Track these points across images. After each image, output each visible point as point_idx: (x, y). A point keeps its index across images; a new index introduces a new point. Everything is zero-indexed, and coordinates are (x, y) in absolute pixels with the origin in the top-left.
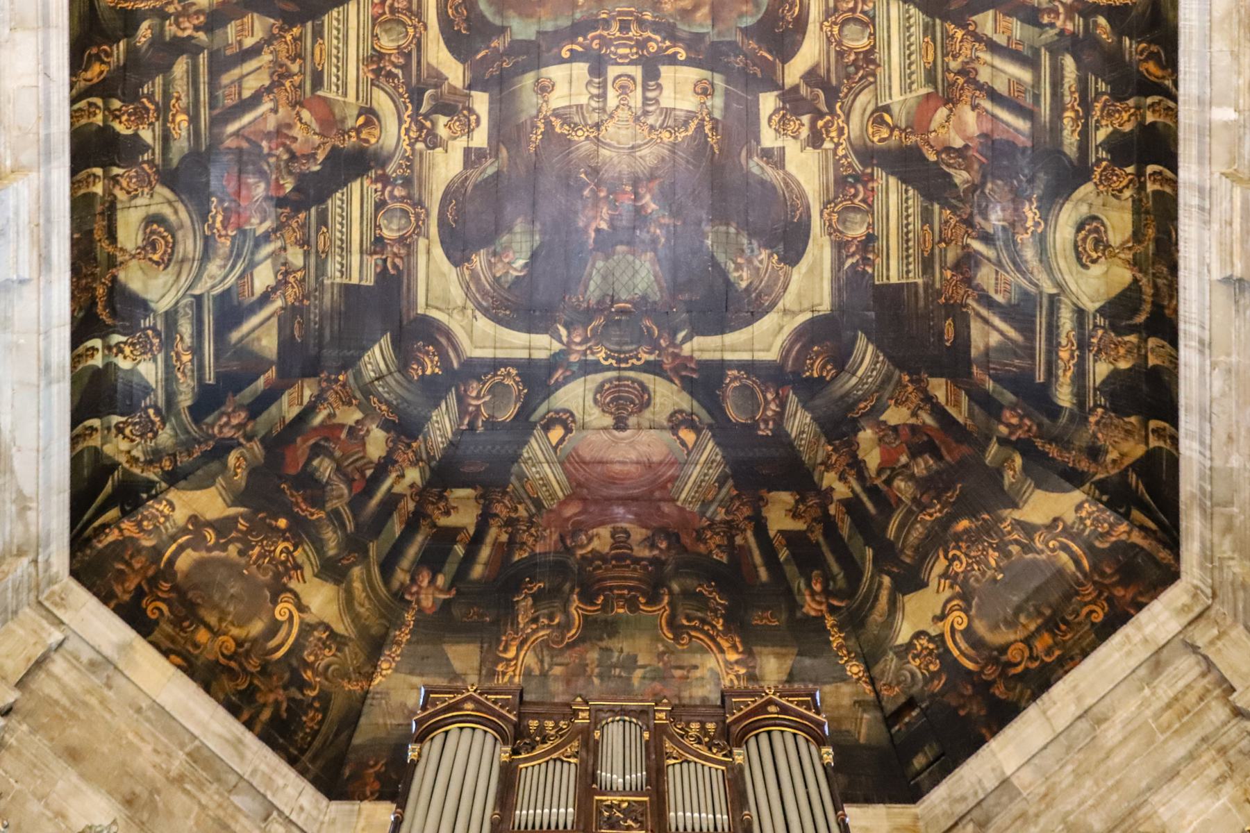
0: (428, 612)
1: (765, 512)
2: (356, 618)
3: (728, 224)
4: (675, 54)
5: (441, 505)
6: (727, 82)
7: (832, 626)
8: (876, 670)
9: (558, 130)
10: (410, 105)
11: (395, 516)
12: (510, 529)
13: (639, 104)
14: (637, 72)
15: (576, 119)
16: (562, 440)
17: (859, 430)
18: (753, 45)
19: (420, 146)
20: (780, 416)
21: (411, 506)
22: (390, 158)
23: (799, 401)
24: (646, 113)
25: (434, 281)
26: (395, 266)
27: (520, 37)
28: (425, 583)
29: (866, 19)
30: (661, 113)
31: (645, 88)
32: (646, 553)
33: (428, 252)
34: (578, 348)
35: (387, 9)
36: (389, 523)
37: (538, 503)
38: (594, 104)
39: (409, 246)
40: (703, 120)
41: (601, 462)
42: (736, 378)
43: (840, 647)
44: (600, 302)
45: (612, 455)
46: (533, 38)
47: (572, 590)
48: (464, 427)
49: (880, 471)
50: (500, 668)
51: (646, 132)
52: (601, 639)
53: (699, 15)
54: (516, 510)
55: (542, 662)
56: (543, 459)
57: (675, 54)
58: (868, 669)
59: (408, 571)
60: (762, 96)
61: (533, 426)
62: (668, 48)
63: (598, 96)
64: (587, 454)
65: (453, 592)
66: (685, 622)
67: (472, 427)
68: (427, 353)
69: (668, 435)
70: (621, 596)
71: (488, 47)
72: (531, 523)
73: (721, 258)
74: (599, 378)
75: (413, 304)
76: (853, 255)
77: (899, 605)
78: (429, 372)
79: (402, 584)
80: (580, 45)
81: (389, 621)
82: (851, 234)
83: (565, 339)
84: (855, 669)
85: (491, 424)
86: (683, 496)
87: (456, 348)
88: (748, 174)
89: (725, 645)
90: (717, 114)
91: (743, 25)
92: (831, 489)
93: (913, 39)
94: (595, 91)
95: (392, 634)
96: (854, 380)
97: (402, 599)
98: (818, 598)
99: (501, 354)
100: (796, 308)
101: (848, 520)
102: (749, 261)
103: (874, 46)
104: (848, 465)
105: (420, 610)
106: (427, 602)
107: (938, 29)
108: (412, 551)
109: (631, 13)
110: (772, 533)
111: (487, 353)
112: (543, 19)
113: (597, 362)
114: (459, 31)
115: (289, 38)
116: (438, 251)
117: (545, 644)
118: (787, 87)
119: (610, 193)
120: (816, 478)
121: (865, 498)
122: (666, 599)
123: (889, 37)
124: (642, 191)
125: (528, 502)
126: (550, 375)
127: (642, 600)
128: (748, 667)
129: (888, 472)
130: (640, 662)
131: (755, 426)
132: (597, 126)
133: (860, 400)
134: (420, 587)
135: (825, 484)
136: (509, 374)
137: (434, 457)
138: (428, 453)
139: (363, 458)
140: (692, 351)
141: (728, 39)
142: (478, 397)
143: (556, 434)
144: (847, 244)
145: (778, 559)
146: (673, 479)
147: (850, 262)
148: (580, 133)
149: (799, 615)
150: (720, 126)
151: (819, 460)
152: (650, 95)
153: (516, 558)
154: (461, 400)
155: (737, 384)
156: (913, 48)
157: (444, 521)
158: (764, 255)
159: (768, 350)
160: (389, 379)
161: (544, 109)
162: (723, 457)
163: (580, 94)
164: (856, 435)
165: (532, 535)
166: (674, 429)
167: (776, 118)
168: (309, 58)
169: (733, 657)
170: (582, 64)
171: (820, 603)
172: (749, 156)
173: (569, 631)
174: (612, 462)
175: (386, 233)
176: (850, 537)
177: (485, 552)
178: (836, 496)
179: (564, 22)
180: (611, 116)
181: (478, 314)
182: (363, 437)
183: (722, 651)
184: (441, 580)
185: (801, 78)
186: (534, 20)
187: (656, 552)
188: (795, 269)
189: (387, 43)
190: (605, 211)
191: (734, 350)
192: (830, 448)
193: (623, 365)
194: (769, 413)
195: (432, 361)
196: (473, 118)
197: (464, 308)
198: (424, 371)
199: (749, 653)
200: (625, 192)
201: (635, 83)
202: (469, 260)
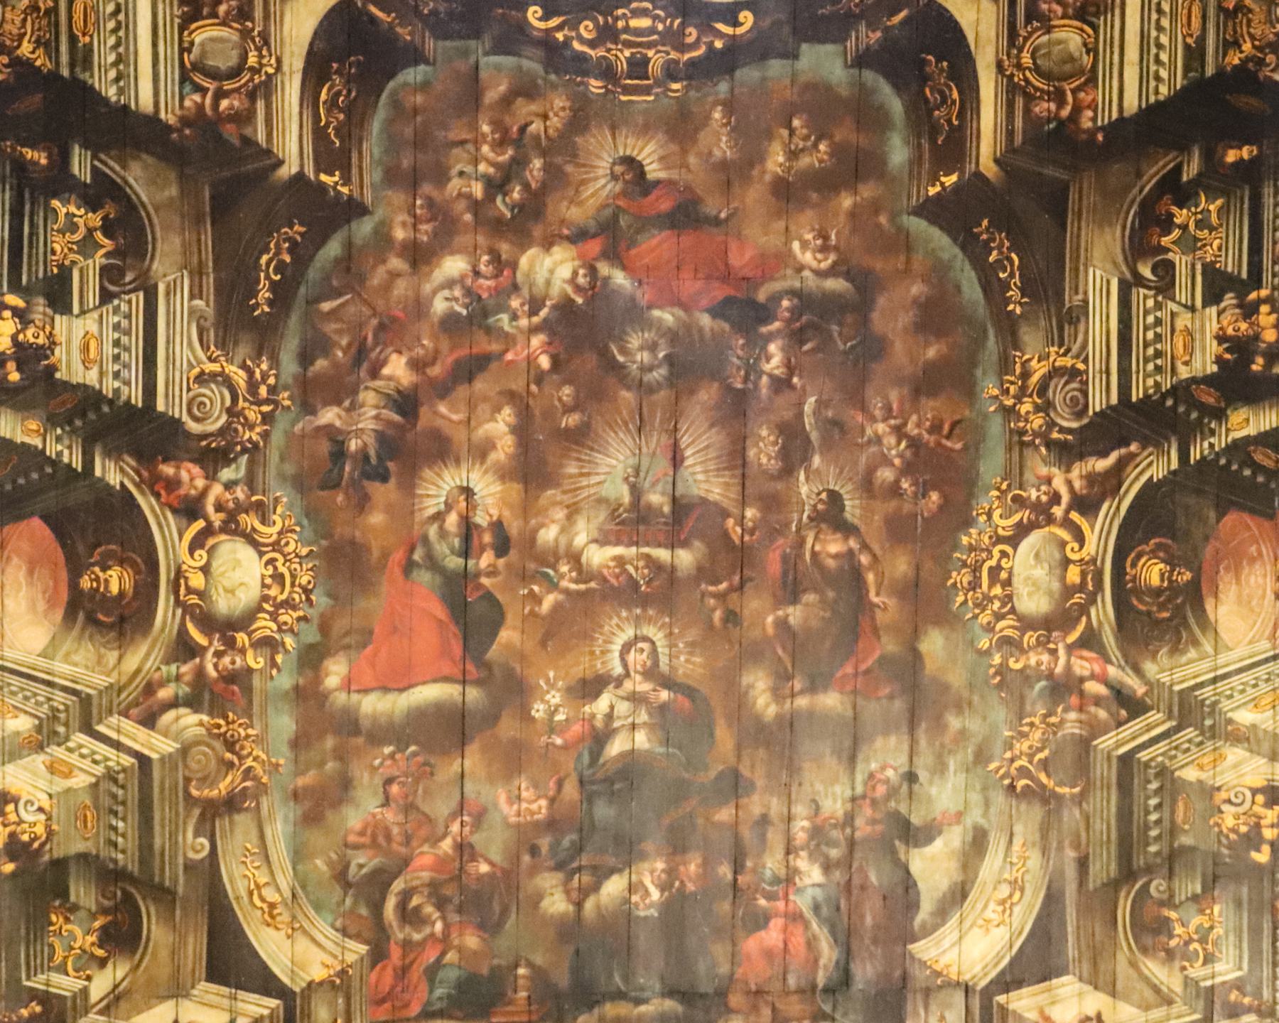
18: (404, 32)
27: (830, 48)
29: (198, 78)
35: (1070, 98)
46: (804, 47)
53: (503, 88)
62: (560, 28)
71: (887, 30)
80: (720, 35)
91: (422, 67)
93: (112, 41)
103: (182, 29)
107: (64, 58)
109: (628, 90)
112: (787, 82)
114: (939, 60)
115: (1247, 47)
123: (155, 45)
141: (448, 43)
156: (111, 25)
168: (1211, 12)
179: (748, 74)
189: (1070, 38)
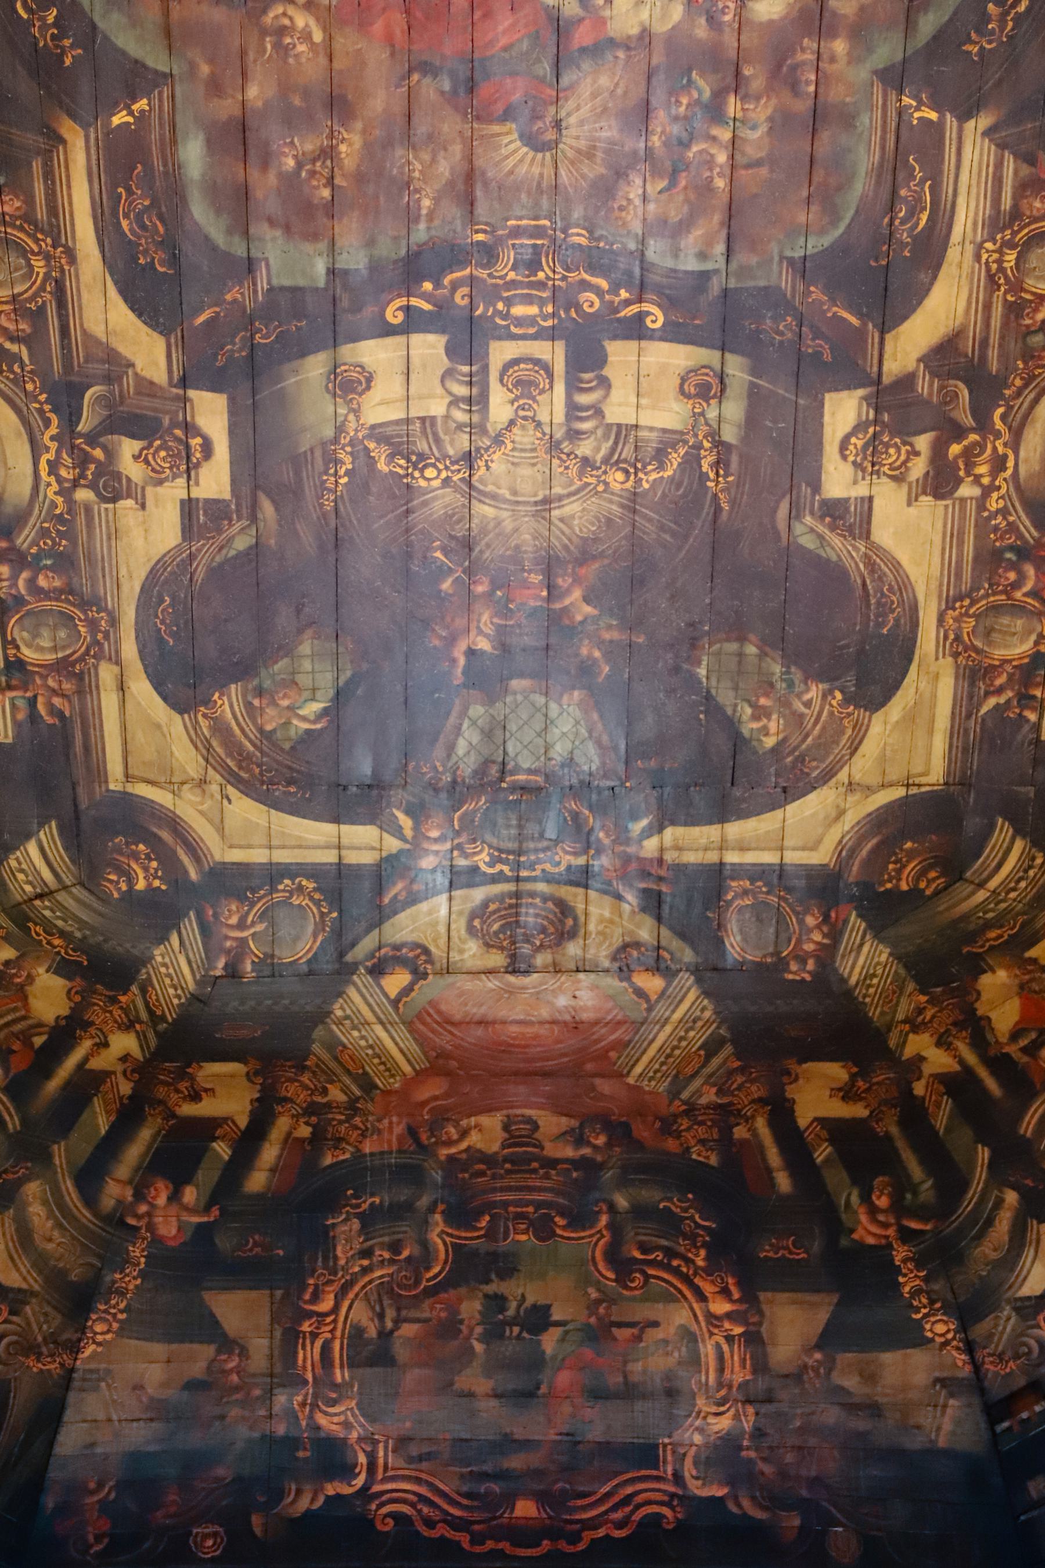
0: (172, 1243)
1: (791, 1091)
2: (40, 1262)
3: (742, 639)
4: (641, 317)
5: (183, 1086)
6: (754, 372)
7: (905, 1261)
8: (979, 1330)
9: (382, 466)
10: (55, 420)
11: (97, 1103)
12: (314, 1119)
13: (559, 417)
14: (555, 353)
15: (422, 446)
16: (407, 990)
17: (984, 972)
19: (83, 495)
20: (827, 955)
21: (126, 1088)
22: (21, 518)
23: (870, 926)
24: (574, 435)
25: (139, 737)
26: (52, 710)
28: (162, 1200)
30: (606, 436)
31: (573, 386)
32: (569, 1152)
33: (122, 688)
34: (435, 847)
36: (85, 1116)
37: (368, 1085)
38: (460, 416)
39: (80, 677)
40: (699, 447)
41: (482, 1022)
42: (745, 892)
43: (916, 1293)
44: (481, 772)
45: (502, 1013)
47: (432, 1209)
48: (218, 973)
49: (1015, 1035)
50: (306, 1327)
51: (574, 471)
52: (488, 1281)
54: (325, 1092)
55: (381, 1316)
56: (369, 1016)
57: (641, 317)
58: (964, 1327)
59: (130, 1182)
60: (830, 399)
61: (351, 969)
63: (470, 400)
64: (454, 1009)
65: (215, 1212)
66: (637, 1255)
67: (233, 973)
68: (135, 855)
69: (613, 983)
70: (521, 1216)
72: (352, 1107)
73: (725, 697)
74: (479, 894)
75: (100, 773)
76: (999, 691)
77: (1031, 1236)
78: (141, 885)
79: (120, 1202)
81: (99, 1257)
82: (999, 653)
83: (408, 833)
84: (940, 1327)
85: (270, 968)
86: (638, 1069)
87: (194, 849)
88: (790, 551)
89: (708, 1288)
90: (729, 435)
92: (922, 1059)
94: (462, 391)
95: (108, 1279)
96: (981, 895)
97: (122, 1223)
98: (881, 1218)
99: (282, 857)
100: (874, 780)
101: (947, 1105)
102: (784, 703)
104: (955, 1024)
105: (157, 1240)
106: (168, 1228)
108: (134, 1152)
110: (802, 1122)
111: (258, 856)
113: (475, 869)
116: (141, 688)
117: (387, 1289)
118: (886, 380)
119: (495, 586)
120: (892, 1043)
121: (983, 1073)
122: (604, 1219)
124: (562, 582)
125: (347, 1081)
126: (379, 889)
127: (560, 1221)
128: (746, 1323)
129: (1033, 1035)
130: (556, 1316)
131: (782, 964)
132: (469, 458)
133: (988, 925)
134: (153, 1206)
135: (909, 1052)
136: (300, 888)
137: (163, 1018)
138: (151, 1012)
139: (24, 1018)
140: (662, 850)
142: (241, 925)
143: (396, 981)
144: (992, 670)
145: (813, 1160)
146: (621, 1045)
147: (992, 701)
148: (430, 473)
149: (844, 1242)
150: (734, 459)
151: (900, 1016)
152: (583, 399)
153: (328, 1160)
154: (205, 930)
155: (748, 901)
157: (188, 1109)
158: (814, 692)
159: (814, 848)
160: (61, 897)
161: (352, 425)
162: (716, 1013)
163: (431, 396)
164: (975, 978)
165: (357, 1128)
166: (624, 972)
167: (857, 442)
169: (721, 1307)
170: (431, 338)
171: (885, 1226)
172: (795, 514)
173: (428, 1269)
174: (504, 1022)
175: (28, 654)
176: (948, 1130)
177: (270, 1153)
178: (927, 1069)
180: (498, 440)
181: (231, 790)
182: (21, 988)
183: (702, 1298)
184: (189, 1195)
185: (919, 360)
186: (323, 246)
187: (586, 1151)
188: (878, 718)
190: (486, 619)
191: (743, 849)
192: (923, 998)
193: (524, 873)
194: (809, 947)
195: (146, 869)
196: (196, 442)
197: (203, 782)
198: (131, 882)
199: (750, 1297)
200: (525, 585)
201: (550, 376)
202: (207, 702)
